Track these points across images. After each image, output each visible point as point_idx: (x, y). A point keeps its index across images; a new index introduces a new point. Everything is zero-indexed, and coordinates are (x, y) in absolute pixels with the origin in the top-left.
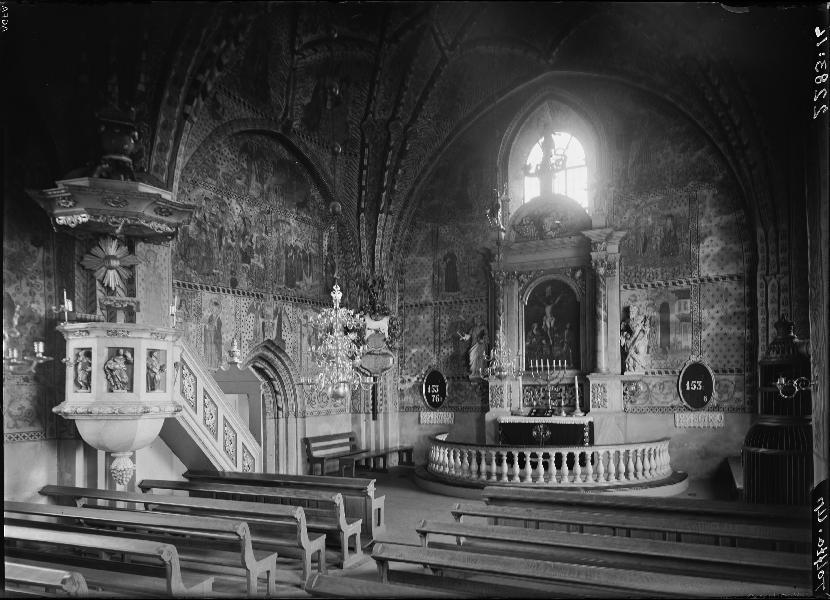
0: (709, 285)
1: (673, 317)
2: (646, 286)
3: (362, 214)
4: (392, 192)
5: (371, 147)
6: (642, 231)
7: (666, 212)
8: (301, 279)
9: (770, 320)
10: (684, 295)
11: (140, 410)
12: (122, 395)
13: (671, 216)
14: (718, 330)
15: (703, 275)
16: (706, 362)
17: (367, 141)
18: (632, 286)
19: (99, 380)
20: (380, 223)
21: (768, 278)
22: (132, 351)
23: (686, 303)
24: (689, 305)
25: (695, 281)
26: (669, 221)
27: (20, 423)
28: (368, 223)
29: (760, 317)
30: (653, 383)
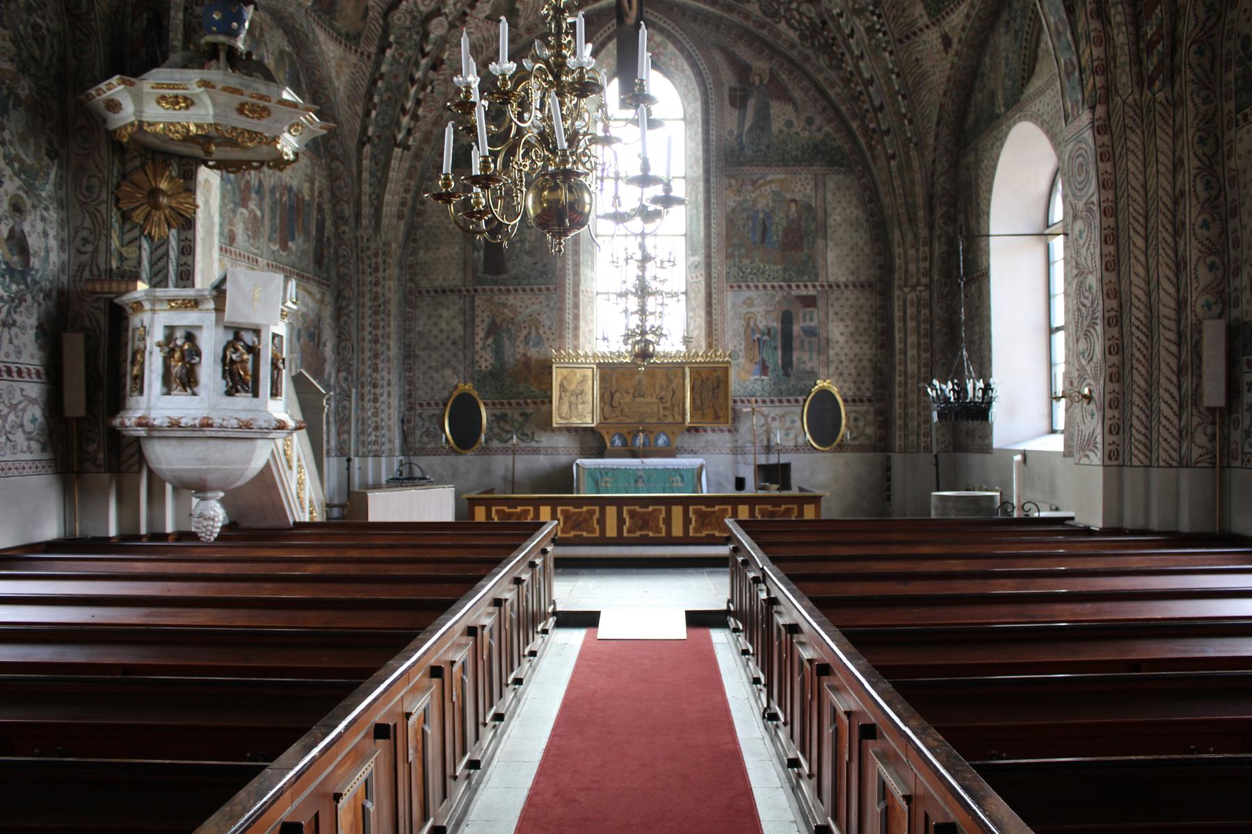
0: (837, 293)
1: (796, 329)
2: (765, 287)
3: (367, 149)
4: (415, 117)
5: (394, 46)
6: (761, 215)
7: (789, 196)
8: (293, 240)
9: (909, 340)
10: (809, 302)
11: (274, 424)
12: (242, 401)
13: (795, 201)
14: (846, 350)
15: (831, 279)
16: (834, 390)
17: (392, 38)
18: (748, 287)
19: (209, 371)
20: (394, 163)
21: (907, 290)
22: (257, 332)
23: (811, 313)
24: (815, 316)
25: (822, 286)
26: (793, 207)
27: (34, 444)
28: (373, 157)
29: (897, 336)
30: (772, 415)
